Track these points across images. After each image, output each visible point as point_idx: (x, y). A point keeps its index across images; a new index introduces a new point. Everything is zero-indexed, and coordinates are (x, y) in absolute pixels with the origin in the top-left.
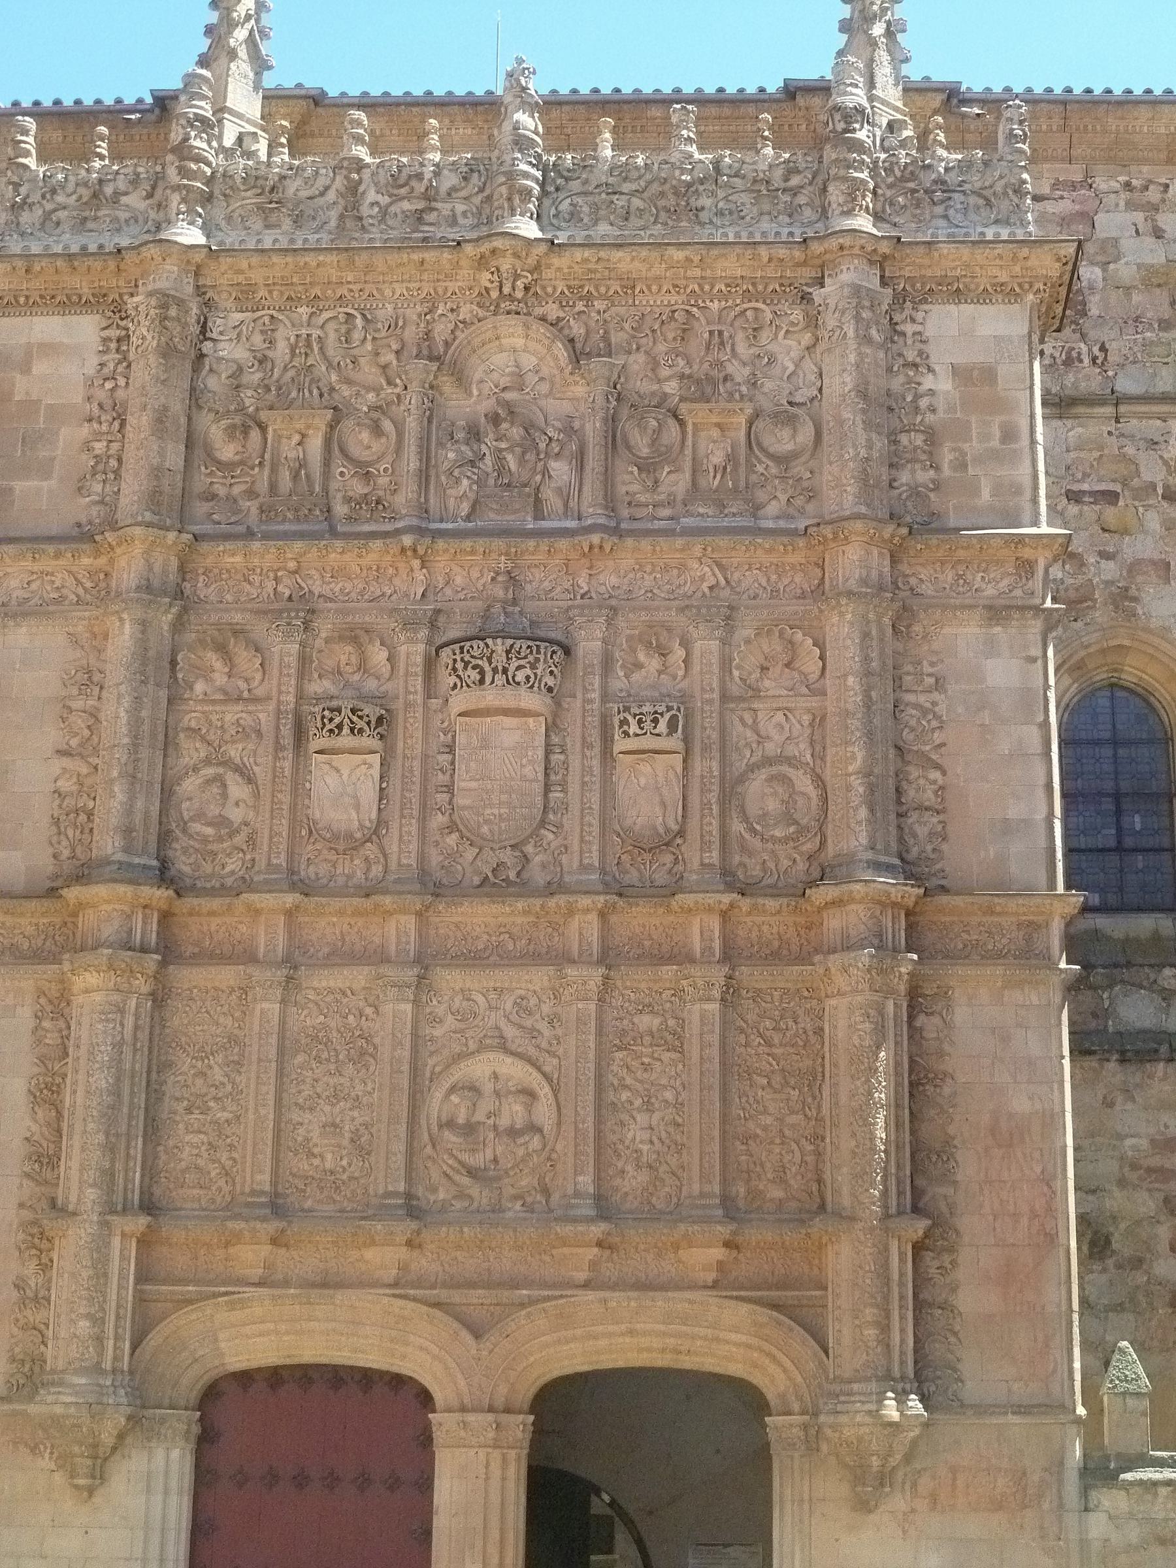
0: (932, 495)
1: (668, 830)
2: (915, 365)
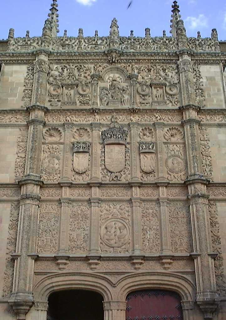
0: (204, 102)
1: (152, 169)
2: (199, 77)
